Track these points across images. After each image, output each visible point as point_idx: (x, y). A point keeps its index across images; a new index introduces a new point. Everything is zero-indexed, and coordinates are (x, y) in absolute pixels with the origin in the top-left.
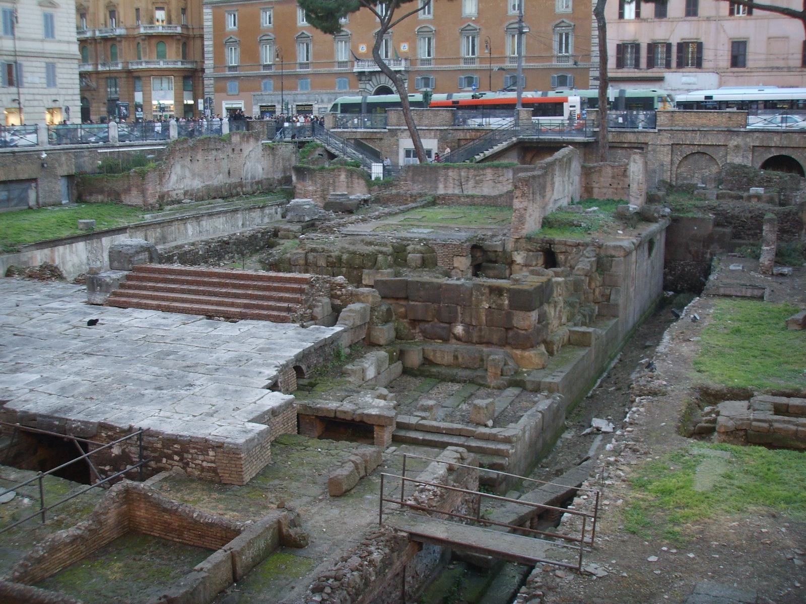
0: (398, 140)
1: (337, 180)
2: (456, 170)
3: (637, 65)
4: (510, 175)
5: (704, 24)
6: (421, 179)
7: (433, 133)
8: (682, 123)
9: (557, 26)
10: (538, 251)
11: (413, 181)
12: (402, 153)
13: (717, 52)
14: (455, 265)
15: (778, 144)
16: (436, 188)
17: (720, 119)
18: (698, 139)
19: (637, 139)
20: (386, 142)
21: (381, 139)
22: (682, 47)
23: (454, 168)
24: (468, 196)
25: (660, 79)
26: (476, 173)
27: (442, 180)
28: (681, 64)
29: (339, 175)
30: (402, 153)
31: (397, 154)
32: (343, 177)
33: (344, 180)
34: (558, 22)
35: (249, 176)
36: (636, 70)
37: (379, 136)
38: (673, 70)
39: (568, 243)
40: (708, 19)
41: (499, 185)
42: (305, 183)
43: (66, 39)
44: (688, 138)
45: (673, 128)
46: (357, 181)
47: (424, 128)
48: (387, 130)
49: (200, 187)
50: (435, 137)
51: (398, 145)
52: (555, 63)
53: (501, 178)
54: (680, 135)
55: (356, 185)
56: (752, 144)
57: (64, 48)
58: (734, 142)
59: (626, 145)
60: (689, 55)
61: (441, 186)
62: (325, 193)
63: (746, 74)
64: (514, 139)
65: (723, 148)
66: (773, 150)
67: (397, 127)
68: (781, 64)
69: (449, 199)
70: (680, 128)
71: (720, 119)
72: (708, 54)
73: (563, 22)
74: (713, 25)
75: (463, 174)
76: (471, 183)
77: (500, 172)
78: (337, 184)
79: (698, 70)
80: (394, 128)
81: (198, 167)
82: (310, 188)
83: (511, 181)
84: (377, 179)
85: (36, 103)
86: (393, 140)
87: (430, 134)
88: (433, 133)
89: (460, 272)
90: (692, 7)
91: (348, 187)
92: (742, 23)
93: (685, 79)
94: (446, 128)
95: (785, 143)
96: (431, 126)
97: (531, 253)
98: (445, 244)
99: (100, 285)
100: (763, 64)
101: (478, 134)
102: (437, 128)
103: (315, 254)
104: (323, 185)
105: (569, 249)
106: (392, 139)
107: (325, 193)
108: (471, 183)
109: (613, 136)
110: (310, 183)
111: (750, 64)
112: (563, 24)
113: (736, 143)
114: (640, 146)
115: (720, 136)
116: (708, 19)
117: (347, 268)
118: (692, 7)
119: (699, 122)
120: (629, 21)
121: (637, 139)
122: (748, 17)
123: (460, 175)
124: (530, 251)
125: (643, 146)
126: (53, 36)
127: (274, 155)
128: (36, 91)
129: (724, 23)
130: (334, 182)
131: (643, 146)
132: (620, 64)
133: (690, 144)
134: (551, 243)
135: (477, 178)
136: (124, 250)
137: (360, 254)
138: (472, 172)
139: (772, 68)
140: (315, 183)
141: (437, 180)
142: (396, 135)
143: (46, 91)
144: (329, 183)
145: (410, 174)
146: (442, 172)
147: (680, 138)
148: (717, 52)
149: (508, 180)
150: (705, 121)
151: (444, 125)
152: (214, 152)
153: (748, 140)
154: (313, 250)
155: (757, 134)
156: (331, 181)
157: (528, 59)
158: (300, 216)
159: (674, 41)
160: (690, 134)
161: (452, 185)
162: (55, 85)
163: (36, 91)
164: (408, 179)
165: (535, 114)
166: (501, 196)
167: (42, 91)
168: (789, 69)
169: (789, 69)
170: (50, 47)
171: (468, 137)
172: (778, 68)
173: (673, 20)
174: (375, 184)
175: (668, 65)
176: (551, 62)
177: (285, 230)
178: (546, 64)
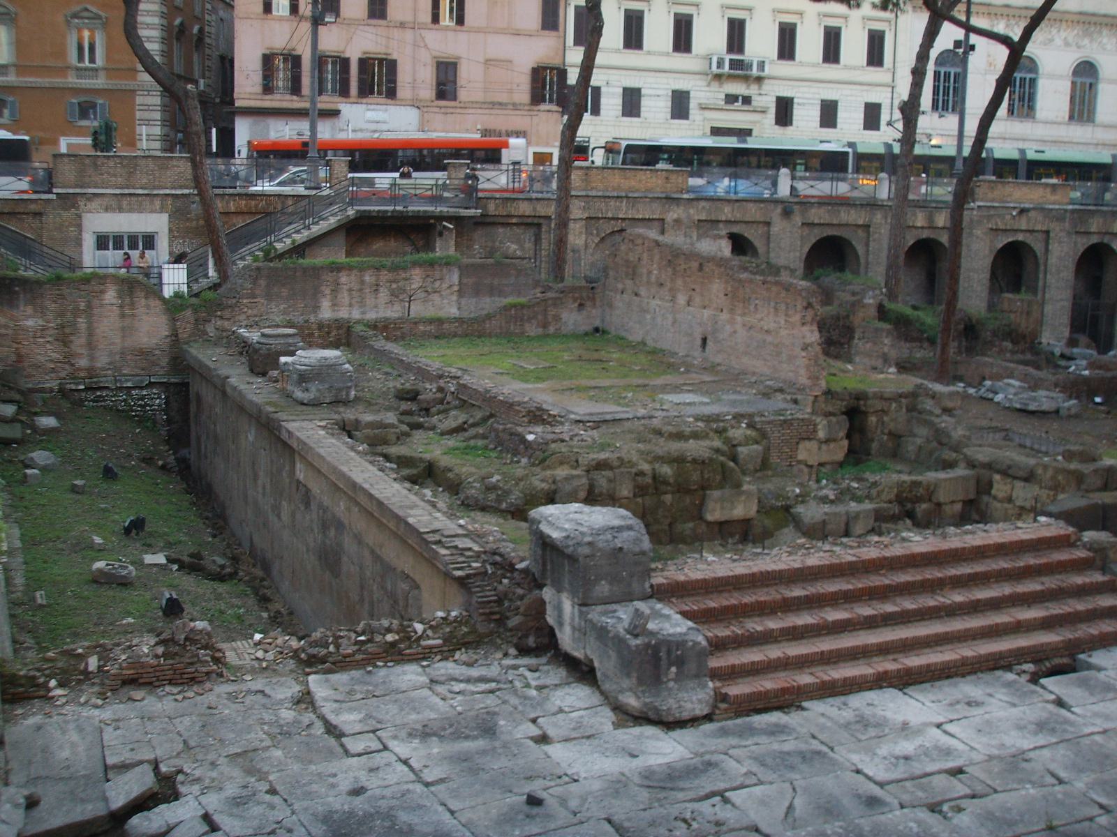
0: (80, 217)
1: (96, 302)
2: (355, 272)
3: (296, 89)
4: (455, 278)
5: (396, 33)
6: (285, 292)
7: (158, 203)
8: (601, 186)
9: (75, 16)
10: (844, 413)
11: (269, 298)
12: (89, 241)
13: (416, 76)
14: (800, 457)
15: (730, 217)
16: (316, 308)
17: (654, 180)
18: (624, 211)
19: (535, 209)
20: (50, 220)
21: (40, 214)
22: (365, 64)
23: (350, 268)
24: (431, 321)
25: (335, 113)
26: (390, 276)
27: (328, 291)
28: (366, 90)
29: (102, 292)
30: (89, 241)
31: (79, 242)
32: (111, 295)
33: (114, 301)
34: (76, 8)
36: (295, 98)
37: (33, 207)
38: (352, 100)
39: (886, 396)
40: (402, 25)
41: (436, 297)
42: (15, 312)
44: (611, 209)
45: (590, 193)
46: (143, 302)
47: (140, 191)
48: (54, 197)
50: (162, 210)
51: (79, 227)
52: (72, 80)
53: (437, 284)
54: (598, 204)
55: (141, 310)
56: (696, 218)
58: (673, 214)
59: (514, 221)
60: (378, 78)
61: (325, 304)
62: (67, 331)
63: (459, 110)
64: (351, 212)
65: (656, 223)
66: (721, 225)
67: (78, 191)
68: (503, 98)
69: (395, 329)
70: (600, 194)
71: (654, 180)
72: (403, 77)
73: (86, 10)
74: (409, 35)
75: (367, 278)
76: (384, 295)
77: (437, 274)
78: (95, 311)
79: (389, 101)
80: (71, 191)
82: (30, 323)
83: (456, 288)
84: (178, 295)
86: (67, 215)
87: (152, 203)
88: (158, 203)
89: (806, 470)
90: (378, 5)
91: (123, 316)
92: (450, 34)
93: (370, 115)
94: (186, 191)
95: (739, 216)
96: (154, 188)
97: (834, 419)
98: (785, 421)
99: (680, 662)
100: (479, 97)
101: (253, 203)
102: (168, 192)
103: (608, 473)
104: (61, 315)
105: (885, 405)
106: (65, 214)
107: (67, 331)
108: (384, 295)
109: (497, 206)
110: (30, 310)
111: (463, 95)
112: (86, 14)
113: (675, 216)
114: (536, 221)
115: (655, 205)
116: (402, 25)
117: (673, 493)
118: (378, 5)
119: (626, 184)
120: (281, 19)
121: (535, 209)
122: (459, 28)
123: (362, 282)
124: (831, 414)
125: (541, 221)
129: (424, 32)
130: (89, 306)
131: (541, 221)
132: (268, 89)
133: (613, 219)
134: (860, 396)
135: (394, 286)
136: (603, 541)
137: (694, 461)
138: (385, 275)
139: (493, 103)
140: (41, 311)
141: (316, 294)
142: (75, 205)
144: (77, 309)
145: (263, 282)
146: (329, 277)
147: (600, 209)
148: (416, 76)
149: (451, 286)
150: (633, 183)
151: (181, 187)
153: (692, 211)
154: (601, 466)
155: (703, 204)
156: (82, 306)
157: (21, 69)
158: (340, 390)
159: (354, 55)
160: (612, 203)
161: (346, 300)
164: (257, 292)
165: (353, 167)
166: (489, 317)
168: (516, 107)
169: (516, 107)
171: (233, 209)
172: (500, 104)
173: (351, 23)
174: (182, 308)
175: (344, 92)
176: (66, 77)
177: (371, 425)
178: (57, 81)
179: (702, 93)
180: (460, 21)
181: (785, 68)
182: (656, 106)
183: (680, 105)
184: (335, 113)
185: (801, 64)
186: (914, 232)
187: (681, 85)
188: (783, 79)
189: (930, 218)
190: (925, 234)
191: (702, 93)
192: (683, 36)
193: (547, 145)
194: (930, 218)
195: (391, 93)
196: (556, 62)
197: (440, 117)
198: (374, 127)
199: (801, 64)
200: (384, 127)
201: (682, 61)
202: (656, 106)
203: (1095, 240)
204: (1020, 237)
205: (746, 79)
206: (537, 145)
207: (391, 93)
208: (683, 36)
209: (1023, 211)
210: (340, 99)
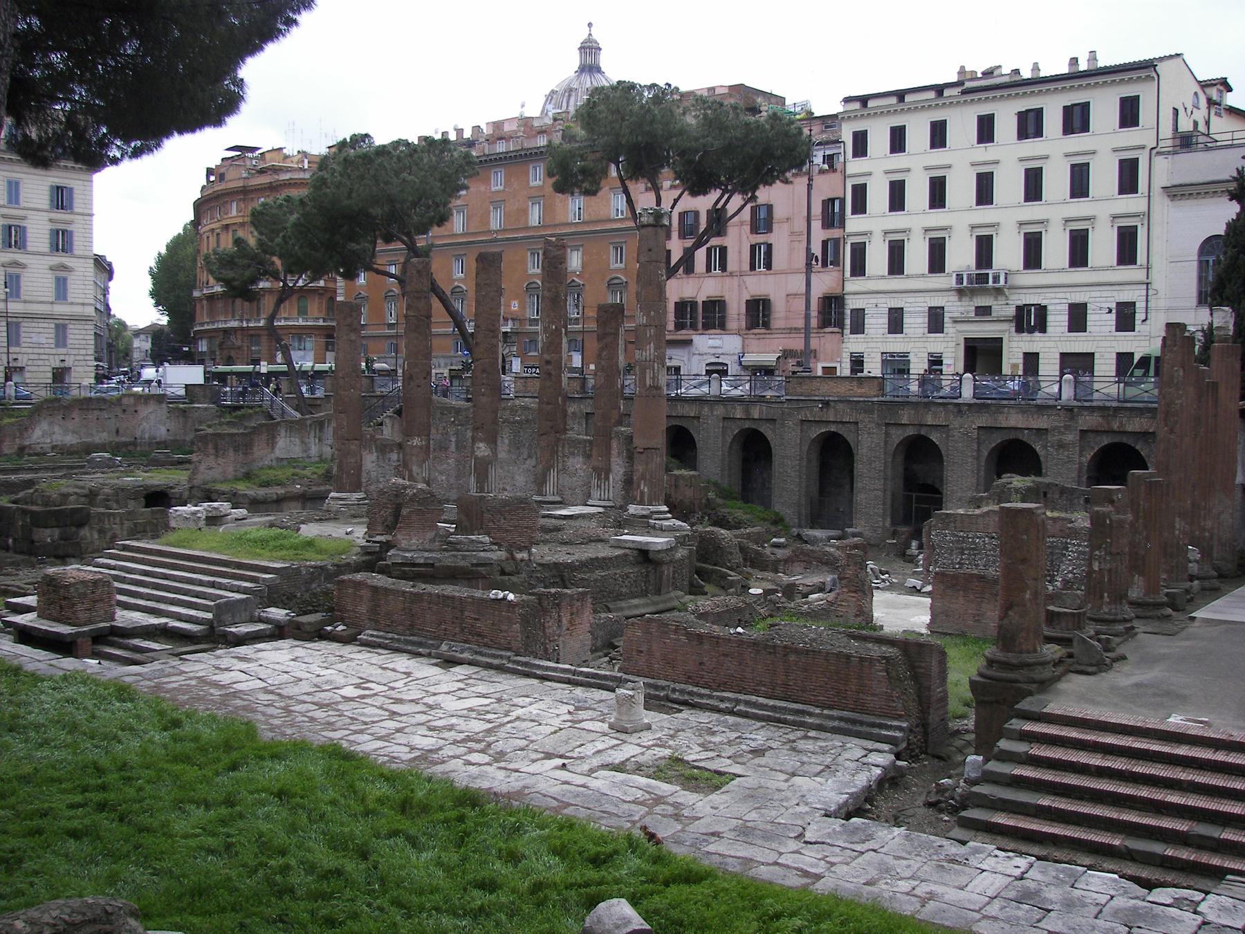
28: (706, 327)
35: (147, 436)
43: (81, 301)
49: (74, 442)
57: (78, 310)
74: (735, 281)
81: (70, 425)
85: (40, 363)
93: (711, 342)
126: (65, 298)
127: (186, 417)
128: (42, 351)
129: (746, 278)
139: (791, 329)
143: (54, 351)
152: (96, 413)
159: (701, 299)
162: (65, 346)
163: (42, 351)
167: (47, 351)
170: (60, 309)
175: (693, 327)
179: (954, 307)
180: (768, 266)
181: (1032, 278)
182: (915, 323)
183: (936, 320)
184: (689, 343)
185: (1094, 269)
186: (739, 423)
187: (937, 302)
188: (1031, 288)
189: (747, 411)
190: (747, 425)
191: (954, 307)
192: (937, 262)
193: (832, 360)
194: (747, 411)
195: (722, 326)
196: (838, 291)
197: (754, 342)
198: (713, 351)
199: (1048, 271)
200: (720, 351)
201: (938, 281)
202: (915, 323)
203: (911, 432)
204: (833, 428)
205: (986, 292)
206: (825, 360)
207: (722, 326)
208: (937, 262)
209: (827, 404)
210: (691, 332)
